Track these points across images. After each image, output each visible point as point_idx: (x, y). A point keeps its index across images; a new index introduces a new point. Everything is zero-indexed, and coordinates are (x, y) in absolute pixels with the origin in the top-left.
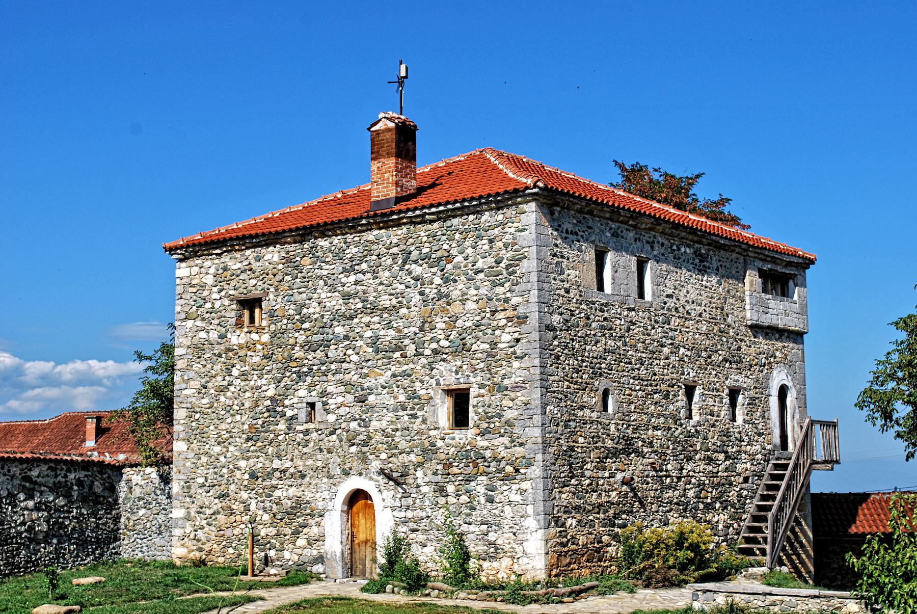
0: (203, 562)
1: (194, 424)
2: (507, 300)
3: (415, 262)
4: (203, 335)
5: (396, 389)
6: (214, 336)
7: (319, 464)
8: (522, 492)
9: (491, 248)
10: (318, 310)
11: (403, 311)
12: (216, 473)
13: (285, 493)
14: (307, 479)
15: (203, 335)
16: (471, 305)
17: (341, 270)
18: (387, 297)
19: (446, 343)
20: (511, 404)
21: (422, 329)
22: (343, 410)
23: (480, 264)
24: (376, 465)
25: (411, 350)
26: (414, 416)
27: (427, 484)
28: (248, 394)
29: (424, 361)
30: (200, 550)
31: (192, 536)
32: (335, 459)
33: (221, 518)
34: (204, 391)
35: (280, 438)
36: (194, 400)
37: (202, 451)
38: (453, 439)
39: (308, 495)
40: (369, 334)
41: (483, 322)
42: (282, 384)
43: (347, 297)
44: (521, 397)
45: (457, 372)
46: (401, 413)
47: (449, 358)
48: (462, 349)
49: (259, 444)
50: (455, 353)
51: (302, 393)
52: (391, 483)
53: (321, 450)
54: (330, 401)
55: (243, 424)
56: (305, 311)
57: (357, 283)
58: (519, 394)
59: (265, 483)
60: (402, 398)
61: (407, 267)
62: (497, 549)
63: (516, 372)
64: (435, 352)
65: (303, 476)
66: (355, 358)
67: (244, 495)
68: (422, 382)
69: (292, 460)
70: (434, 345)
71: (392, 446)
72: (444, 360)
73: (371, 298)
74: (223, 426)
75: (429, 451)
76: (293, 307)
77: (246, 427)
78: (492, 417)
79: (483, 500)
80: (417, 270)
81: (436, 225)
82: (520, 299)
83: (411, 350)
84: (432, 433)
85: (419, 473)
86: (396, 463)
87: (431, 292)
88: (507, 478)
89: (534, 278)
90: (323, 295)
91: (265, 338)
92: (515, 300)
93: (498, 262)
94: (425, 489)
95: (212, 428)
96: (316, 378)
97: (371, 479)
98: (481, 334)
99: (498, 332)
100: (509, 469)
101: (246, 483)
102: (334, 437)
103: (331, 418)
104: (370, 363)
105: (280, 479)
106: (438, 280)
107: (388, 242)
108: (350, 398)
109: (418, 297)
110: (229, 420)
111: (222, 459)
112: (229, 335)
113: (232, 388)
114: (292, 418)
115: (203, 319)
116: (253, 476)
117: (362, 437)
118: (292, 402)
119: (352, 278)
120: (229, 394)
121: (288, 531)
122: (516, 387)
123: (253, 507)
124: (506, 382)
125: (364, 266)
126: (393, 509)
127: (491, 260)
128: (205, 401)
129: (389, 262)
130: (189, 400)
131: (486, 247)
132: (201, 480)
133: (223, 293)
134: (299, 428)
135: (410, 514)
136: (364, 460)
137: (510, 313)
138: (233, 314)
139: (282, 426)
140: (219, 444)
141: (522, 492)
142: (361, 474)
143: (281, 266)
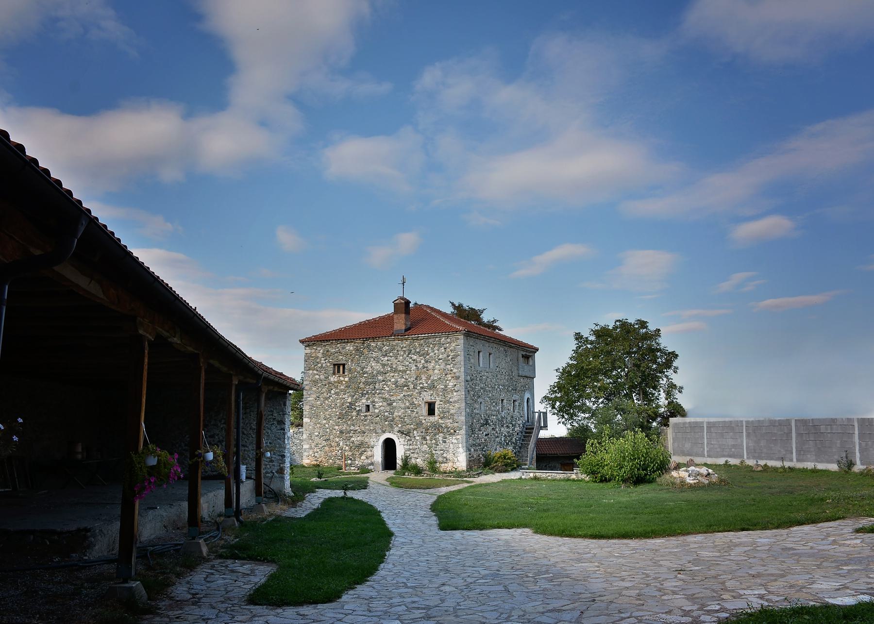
0: (319, 465)
1: (313, 412)
2: (451, 370)
3: (414, 354)
4: (317, 377)
5: (405, 401)
6: (322, 377)
7: (372, 428)
8: (457, 439)
9: (445, 351)
10: (371, 370)
11: (408, 372)
12: (324, 431)
13: (356, 439)
14: (366, 434)
15: (317, 377)
16: (436, 371)
17: (381, 355)
18: (400, 366)
19: (427, 385)
20: (453, 408)
21: (416, 379)
22: (382, 408)
23: (440, 357)
24: (396, 429)
25: (412, 386)
26: (413, 411)
27: (418, 436)
28: (338, 401)
29: (417, 391)
30: (317, 461)
31: (313, 455)
32: (378, 426)
33: (327, 448)
34: (318, 399)
35: (354, 418)
36: (313, 402)
37: (317, 422)
38: (430, 420)
39: (367, 440)
40: (393, 380)
41: (442, 378)
42: (355, 398)
43: (384, 365)
44: (457, 405)
45: (431, 396)
46: (407, 410)
47: (428, 390)
48: (432, 387)
49: (344, 420)
50: (430, 389)
51: (364, 401)
52: (404, 435)
53: (372, 423)
54: (376, 405)
55: (337, 412)
56: (365, 370)
57: (388, 360)
58: (456, 404)
59: (346, 435)
60: (407, 404)
61: (410, 356)
62: (447, 459)
63: (455, 396)
64: (422, 388)
65: (364, 433)
66: (387, 389)
67: (337, 440)
68: (416, 398)
69: (359, 426)
70: (421, 385)
71: (403, 422)
72: (425, 391)
73: (394, 367)
74: (327, 413)
75: (419, 424)
76: (359, 368)
77: (338, 413)
78: (445, 412)
79: (441, 442)
80: (415, 357)
81: (422, 341)
82: (457, 370)
83: (412, 386)
84: (422, 417)
85: (415, 432)
86: (404, 429)
87: (420, 366)
88: (451, 434)
89: (462, 363)
90: (373, 364)
91: (347, 379)
92: (455, 370)
93: (448, 356)
94: (417, 438)
95: (322, 413)
96: (370, 396)
97: (395, 434)
98: (441, 382)
99: (447, 382)
100: (452, 431)
101: (338, 435)
102: (378, 418)
103: (377, 411)
104: (394, 391)
105: (354, 433)
106: (423, 361)
107: (402, 346)
108: (385, 404)
109: (415, 367)
110: (330, 411)
111: (327, 425)
112: (330, 378)
113: (331, 398)
114: (359, 410)
115: (317, 370)
116: (341, 432)
117: (390, 418)
118: (359, 404)
119: (386, 358)
120: (330, 400)
121: (358, 453)
122: (455, 402)
123: (341, 444)
124: (451, 400)
125: (391, 354)
126: (404, 445)
127: (445, 355)
128: (319, 403)
129: (402, 353)
130: (311, 402)
131: (443, 351)
132: (317, 434)
133: (327, 361)
134: (362, 414)
135: (411, 447)
136: (392, 427)
137: (453, 375)
138: (332, 369)
139: (354, 413)
140: (325, 420)
141: (457, 439)
142: (390, 432)
143: (354, 352)
